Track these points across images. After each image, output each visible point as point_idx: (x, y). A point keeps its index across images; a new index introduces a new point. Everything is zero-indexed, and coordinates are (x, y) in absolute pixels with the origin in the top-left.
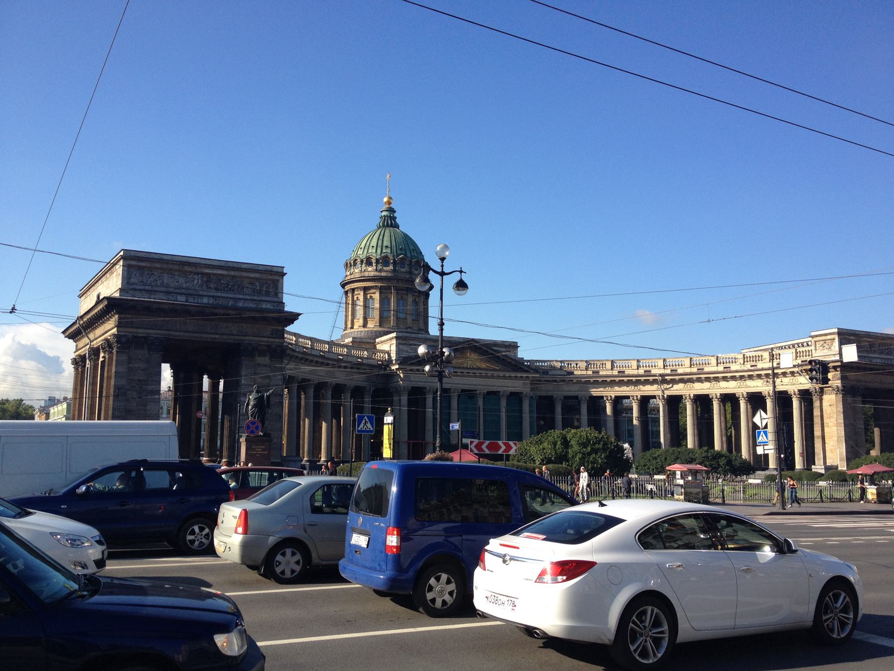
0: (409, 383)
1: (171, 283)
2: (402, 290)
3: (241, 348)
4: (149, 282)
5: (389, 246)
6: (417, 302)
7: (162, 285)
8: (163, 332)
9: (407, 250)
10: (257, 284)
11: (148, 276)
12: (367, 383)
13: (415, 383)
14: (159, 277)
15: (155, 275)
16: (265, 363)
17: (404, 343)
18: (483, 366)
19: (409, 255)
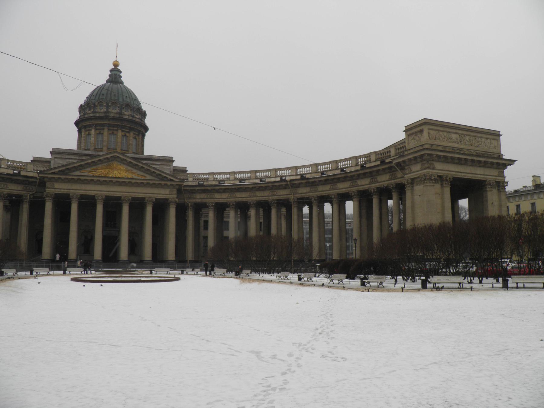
2: (114, 126)
6: (128, 136)
12: (25, 192)
13: (58, 190)
17: (60, 157)
18: (129, 177)
19: (121, 100)
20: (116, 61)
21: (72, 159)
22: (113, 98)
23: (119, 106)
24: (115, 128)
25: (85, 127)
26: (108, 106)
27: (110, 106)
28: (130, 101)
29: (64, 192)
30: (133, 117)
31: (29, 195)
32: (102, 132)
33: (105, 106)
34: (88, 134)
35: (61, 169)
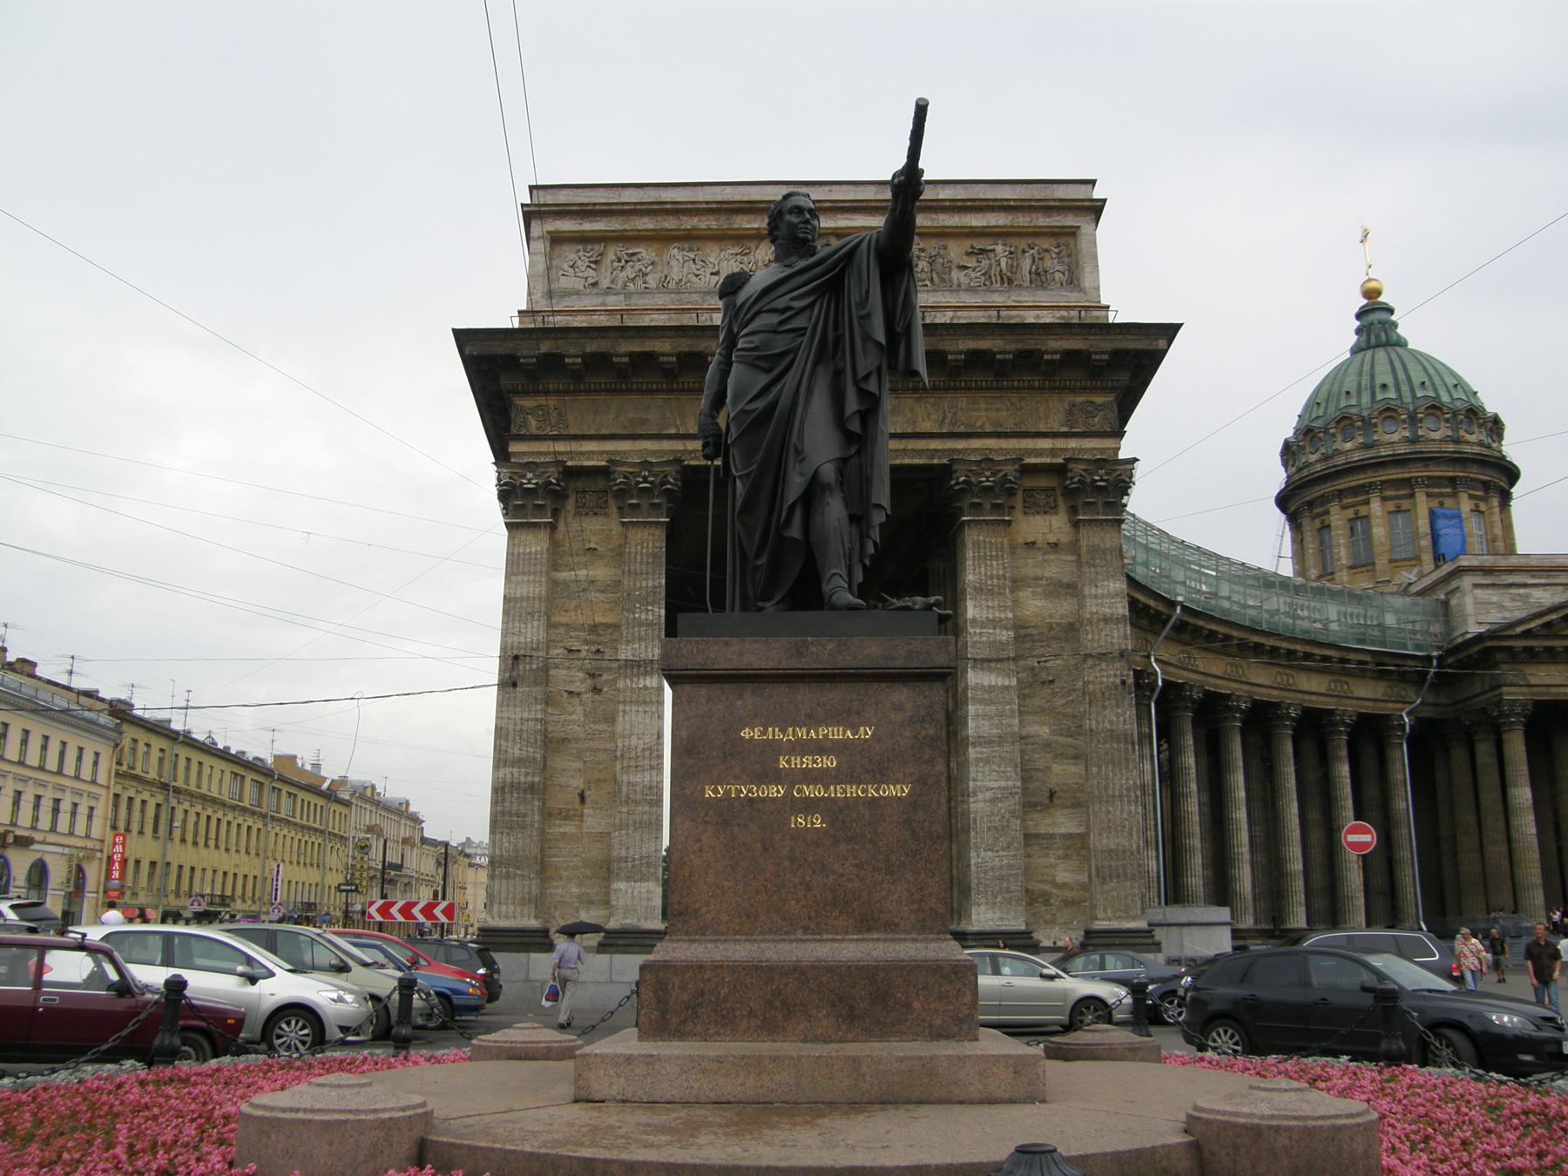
0: (1525, 690)
1: (695, 280)
3: (953, 483)
4: (620, 285)
5: (1389, 381)
6: (1483, 513)
7: (663, 286)
8: (666, 445)
9: (1439, 387)
10: (999, 248)
11: (616, 264)
12: (1390, 705)
14: (653, 263)
15: (639, 260)
16: (1053, 539)
17: (1489, 582)
19: (1445, 398)
20: (1370, 280)
21: (1525, 585)
22: (1419, 394)
23: (1447, 416)
24: (1444, 490)
25: (1341, 494)
26: (1413, 420)
27: (1421, 420)
28: (1467, 396)
29: (1559, 694)
30: (1489, 447)
31: (1408, 714)
32: (1406, 504)
33: (1404, 421)
34: (1353, 516)
35: (1547, 618)
